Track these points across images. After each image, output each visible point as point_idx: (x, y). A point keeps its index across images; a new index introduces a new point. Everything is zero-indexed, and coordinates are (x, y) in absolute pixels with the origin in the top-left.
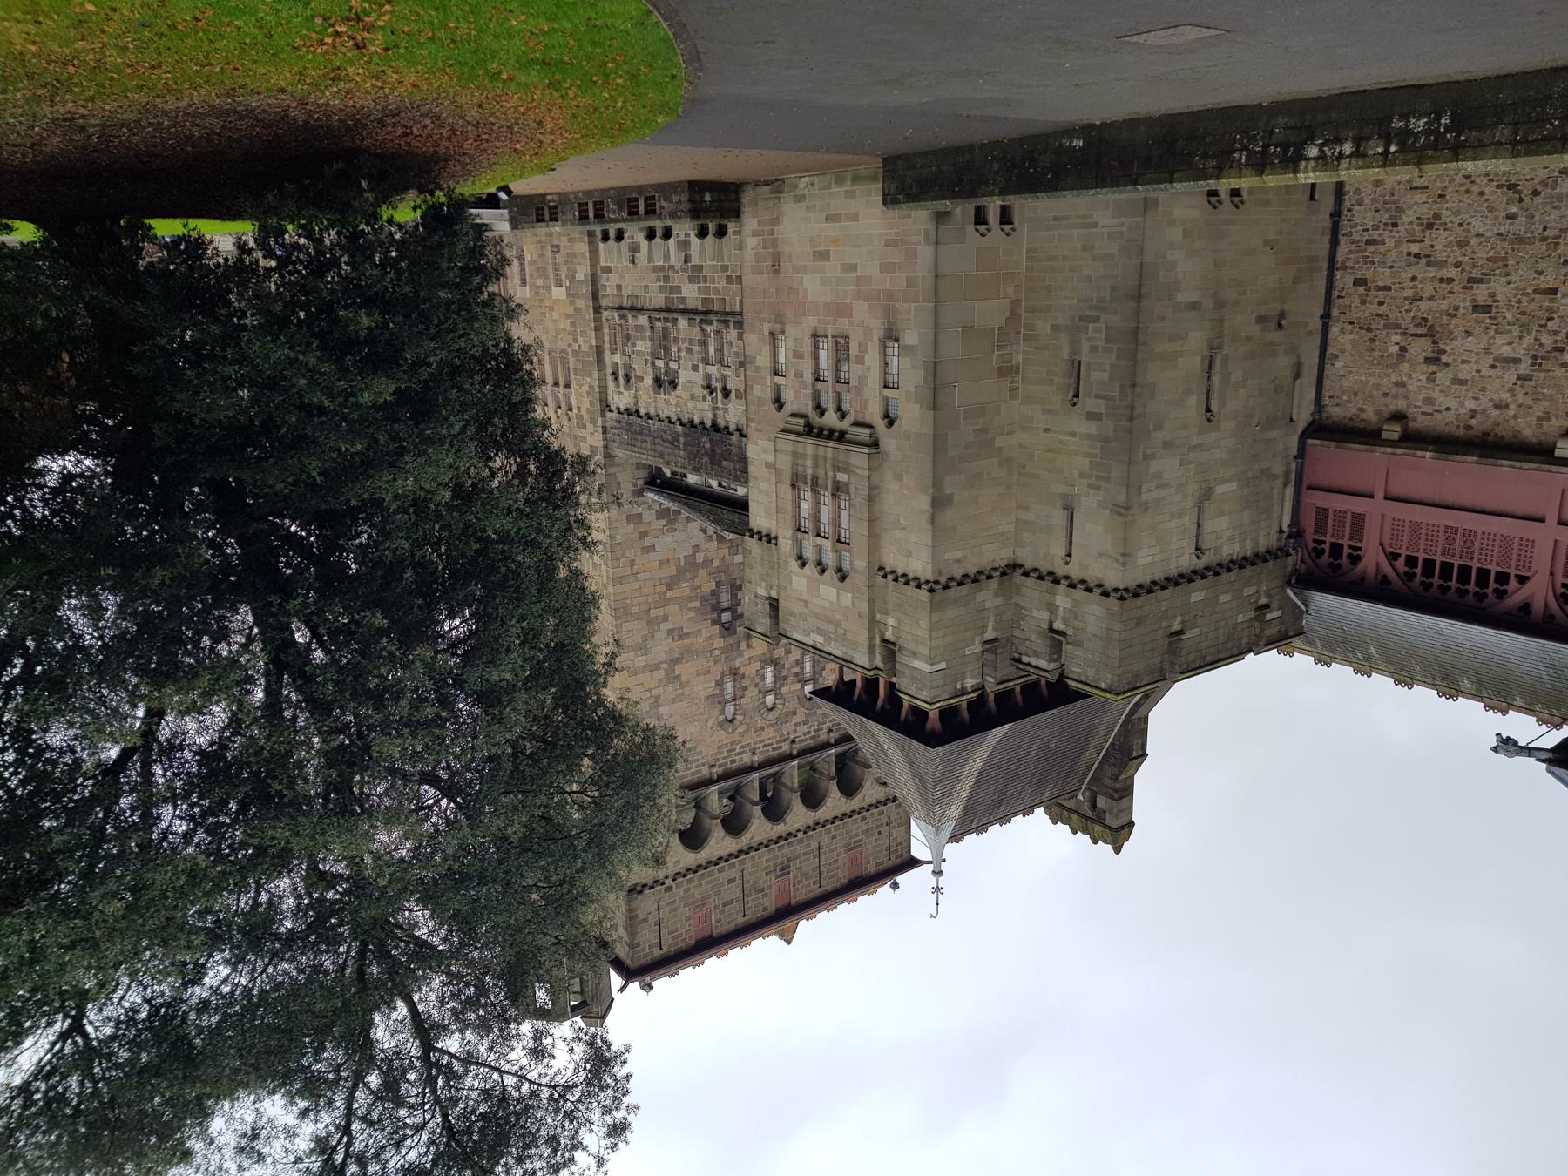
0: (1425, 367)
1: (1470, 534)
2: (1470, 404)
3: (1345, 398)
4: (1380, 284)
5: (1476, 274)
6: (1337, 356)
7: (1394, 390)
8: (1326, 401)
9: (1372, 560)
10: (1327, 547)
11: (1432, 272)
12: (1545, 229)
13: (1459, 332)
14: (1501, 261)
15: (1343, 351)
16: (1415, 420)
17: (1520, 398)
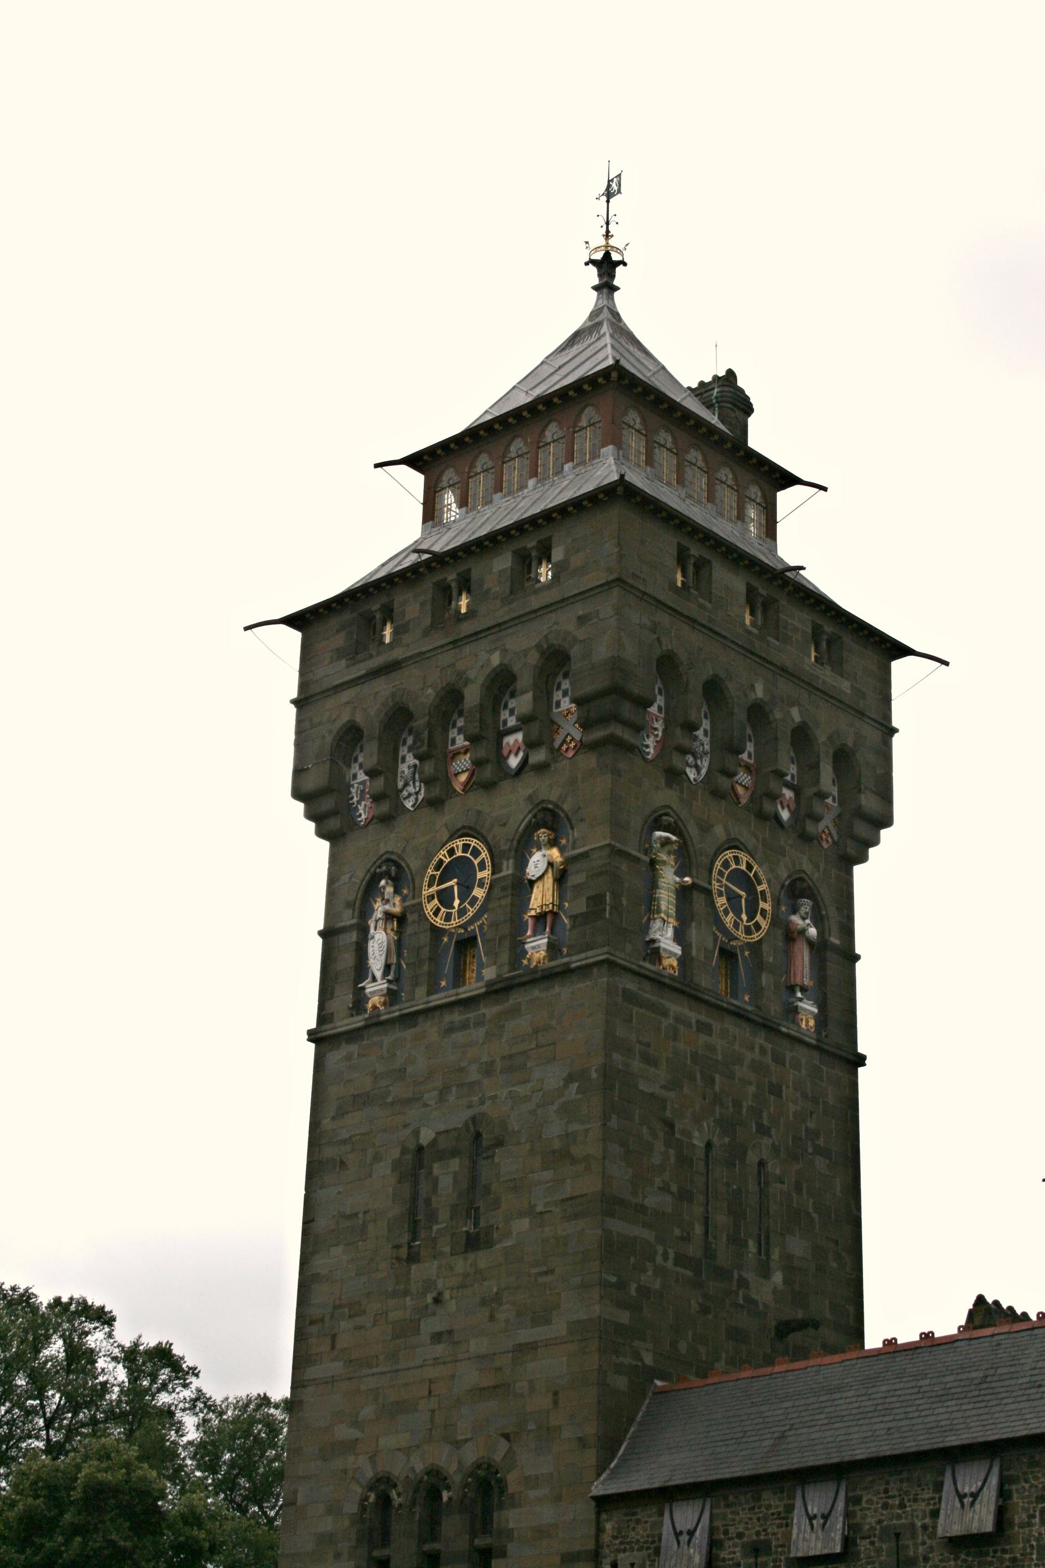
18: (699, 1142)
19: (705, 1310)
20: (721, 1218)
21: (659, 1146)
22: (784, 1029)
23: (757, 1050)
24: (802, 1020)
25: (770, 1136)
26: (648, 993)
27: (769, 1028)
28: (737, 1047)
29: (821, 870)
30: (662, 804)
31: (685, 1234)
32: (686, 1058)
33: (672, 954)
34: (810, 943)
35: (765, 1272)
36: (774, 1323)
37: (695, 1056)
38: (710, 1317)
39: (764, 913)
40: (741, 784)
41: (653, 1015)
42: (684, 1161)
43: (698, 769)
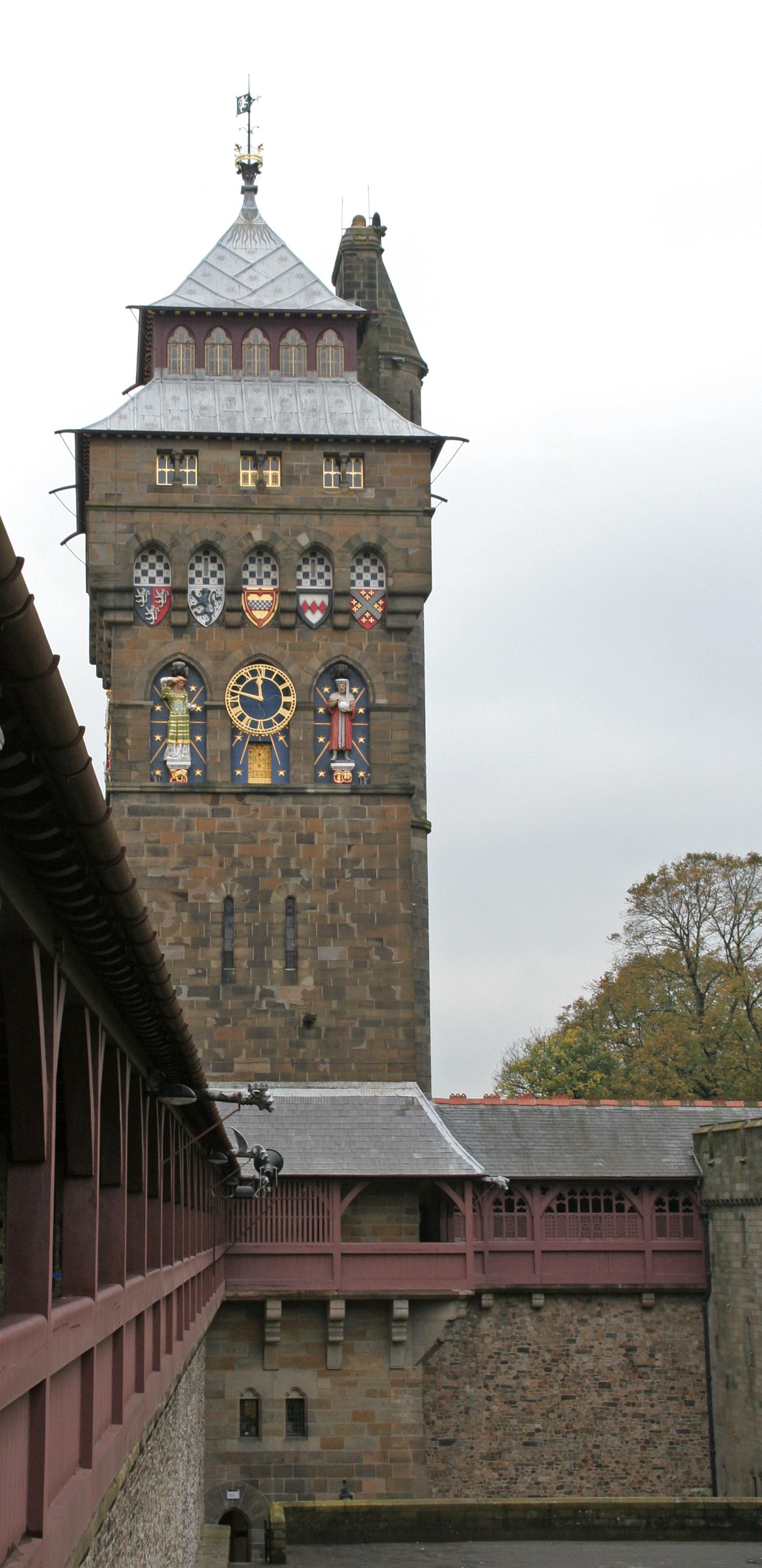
0: (636, 1344)
1: (586, 1234)
2: (602, 1321)
3: (688, 1318)
4: (675, 1402)
5: (612, 1409)
6: (698, 1349)
7: (654, 1326)
8: (701, 1315)
9: (646, 1204)
10: (681, 1207)
11: (641, 1410)
12: (575, 1438)
13: (617, 1370)
14: (599, 1417)
15: (694, 1353)
16: (636, 1307)
17: (572, 1327)
18: (215, 899)
19: (222, 1022)
20: (242, 952)
21: (170, 914)
22: (309, 791)
23: (283, 813)
24: (336, 777)
25: (300, 876)
26: (158, 802)
27: (298, 793)
28: (259, 818)
29: (364, 648)
30: (171, 653)
31: (200, 971)
32: (201, 841)
33: (179, 768)
34: (348, 714)
35: (292, 979)
36: (302, 1016)
37: (209, 838)
38: (229, 1026)
39: (287, 706)
40: (260, 609)
41: (162, 818)
42: (199, 917)
43: (210, 614)
